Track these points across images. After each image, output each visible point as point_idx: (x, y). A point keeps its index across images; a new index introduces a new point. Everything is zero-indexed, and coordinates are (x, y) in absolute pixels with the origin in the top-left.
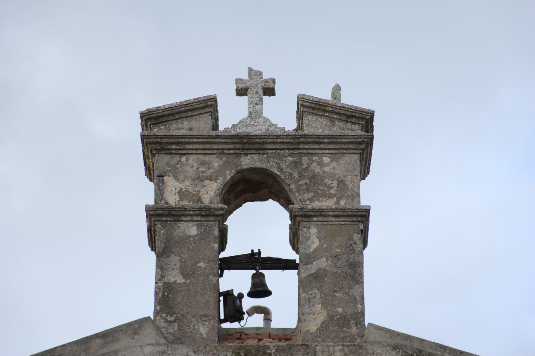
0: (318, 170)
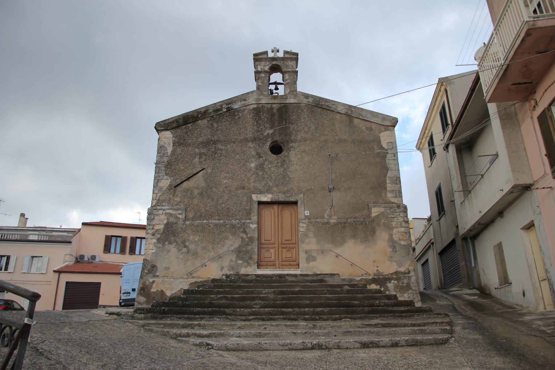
0: (288, 64)
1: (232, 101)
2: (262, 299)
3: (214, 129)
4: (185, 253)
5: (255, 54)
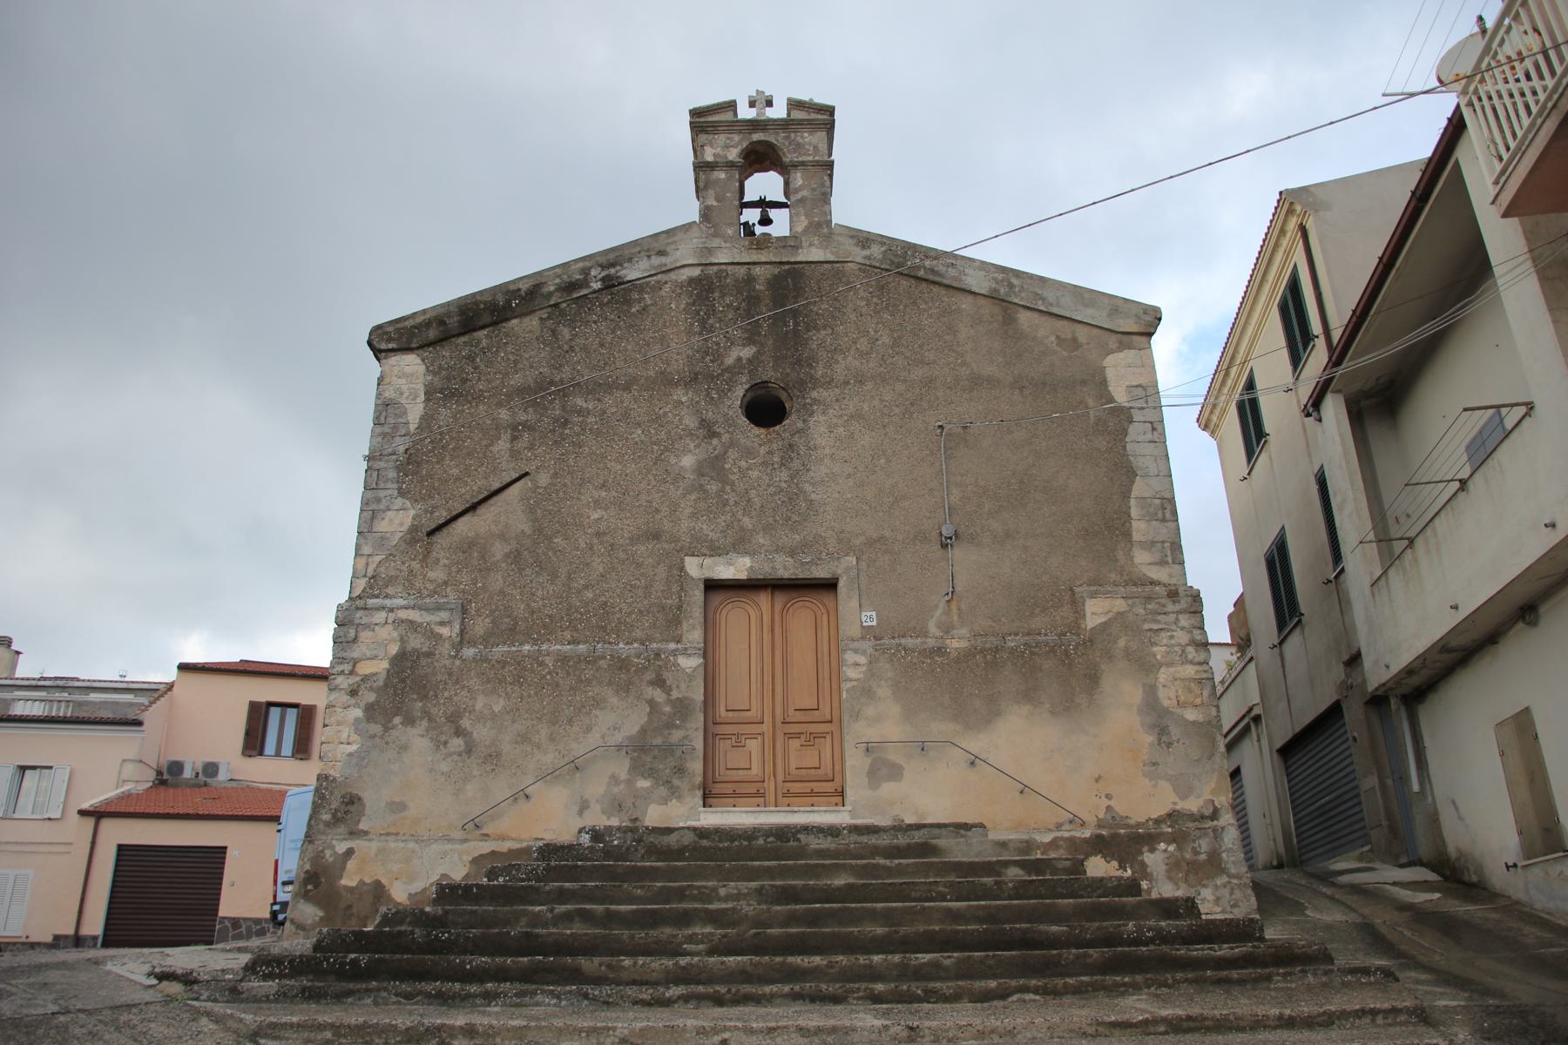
0: (801, 141)
1: (621, 256)
2: (715, 918)
3: (559, 347)
4: (460, 754)
5: (695, 109)
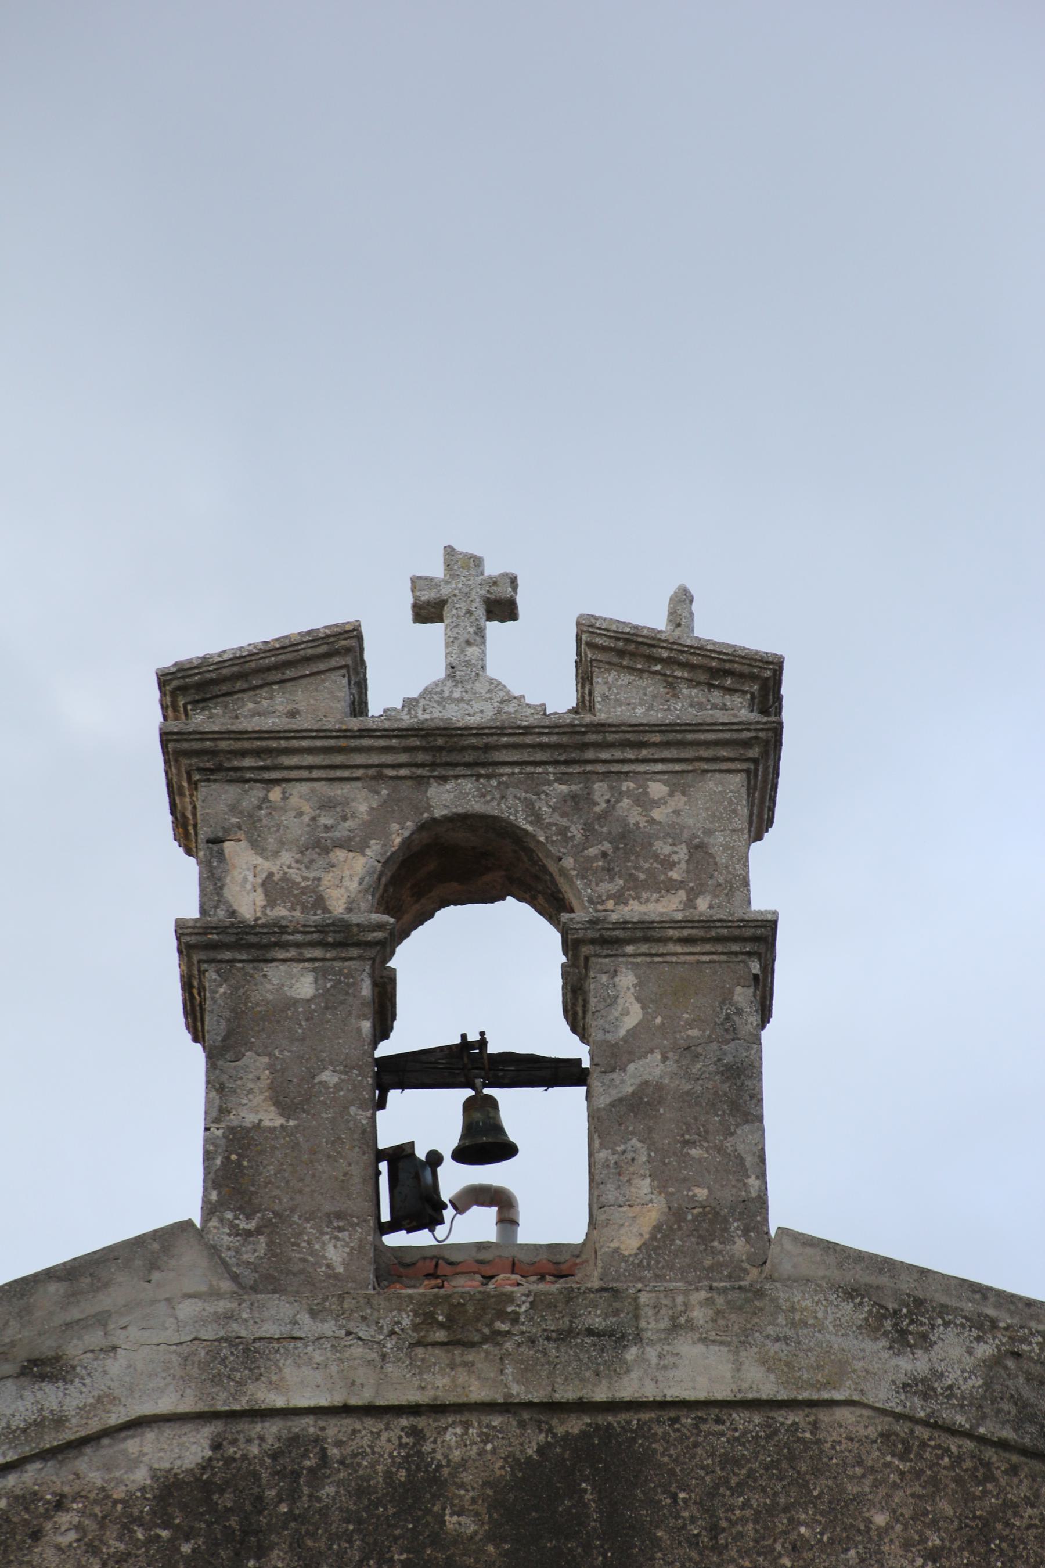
0: (635, 817)
